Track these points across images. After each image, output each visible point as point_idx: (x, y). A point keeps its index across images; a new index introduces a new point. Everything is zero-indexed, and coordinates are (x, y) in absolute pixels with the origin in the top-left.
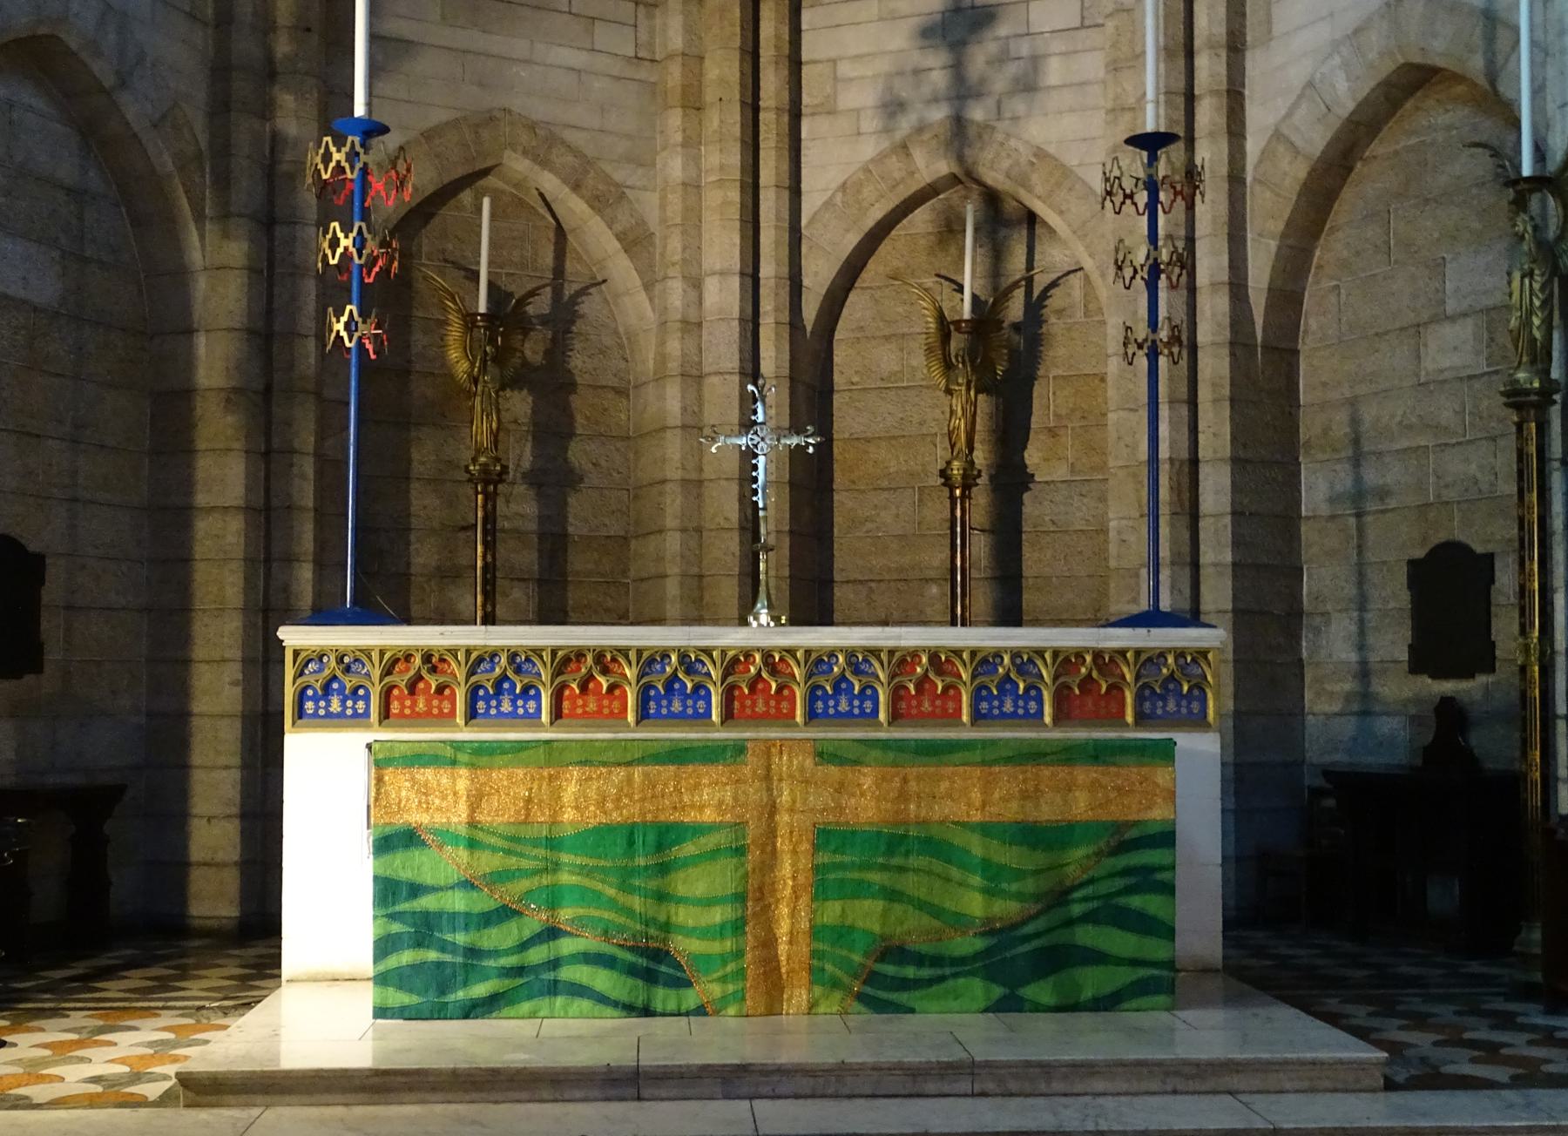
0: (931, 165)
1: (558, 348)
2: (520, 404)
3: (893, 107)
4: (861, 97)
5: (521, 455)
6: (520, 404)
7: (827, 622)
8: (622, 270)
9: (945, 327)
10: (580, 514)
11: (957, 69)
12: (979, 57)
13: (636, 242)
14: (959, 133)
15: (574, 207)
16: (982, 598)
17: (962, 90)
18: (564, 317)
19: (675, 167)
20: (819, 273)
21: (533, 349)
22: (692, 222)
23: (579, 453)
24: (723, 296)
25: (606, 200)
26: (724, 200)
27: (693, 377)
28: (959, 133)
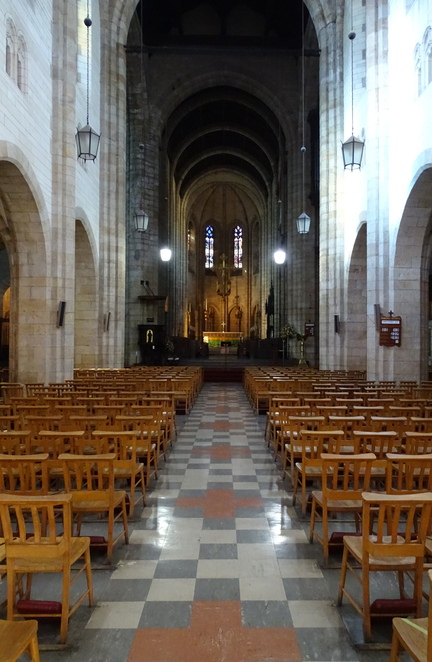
0: (235, 305)
1: (214, 316)
2: (212, 319)
3: (233, 301)
4: (231, 301)
5: (212, 322)
6: (212, 319)
7: (230, 331)
8: (217, 311)
9: (236, 315)
10: (215, 325)
11: (237, 300)
12: (238, 299)
13: (218, 309)
14: (237, 303)
15: (215, 308)
16: (238, 330)
17: (237, 301)
18: (214, 313)
19: (220, 305)
20: (229, 311)
21: (212, 315)
22: (222, 308)
23: (215, 322)
24: (223, 313)
25: (217, 307)
26: (223, 307)
27: (222, 317)
28: (237, 303)
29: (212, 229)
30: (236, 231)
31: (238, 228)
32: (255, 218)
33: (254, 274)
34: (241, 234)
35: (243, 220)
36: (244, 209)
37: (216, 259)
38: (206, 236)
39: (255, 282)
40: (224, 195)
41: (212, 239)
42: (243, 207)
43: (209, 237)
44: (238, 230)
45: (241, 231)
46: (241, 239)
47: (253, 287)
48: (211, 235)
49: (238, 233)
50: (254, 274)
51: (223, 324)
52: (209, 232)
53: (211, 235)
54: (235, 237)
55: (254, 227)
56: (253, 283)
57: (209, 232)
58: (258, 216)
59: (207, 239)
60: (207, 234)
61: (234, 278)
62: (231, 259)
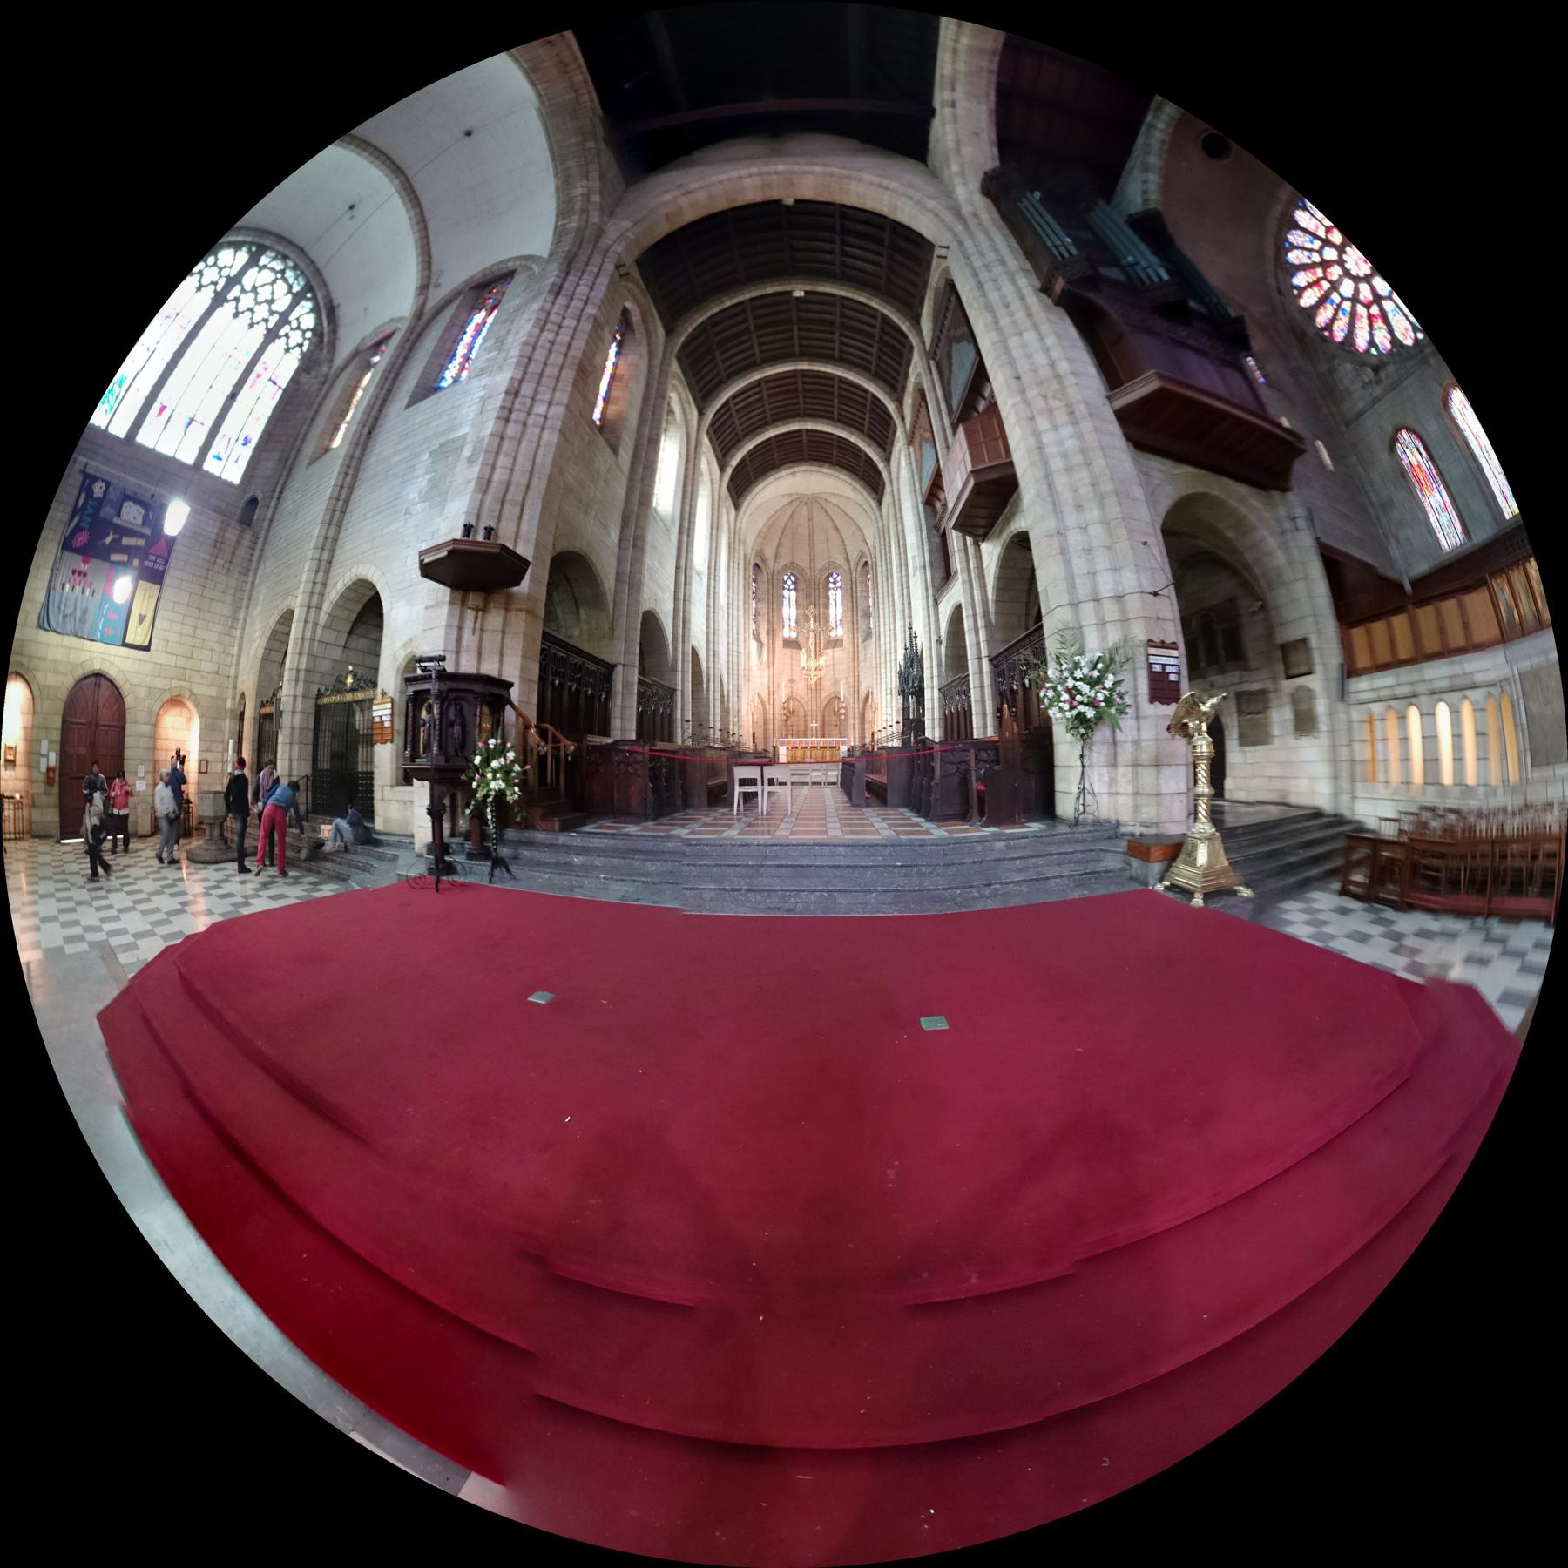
29: (793, 579)
30: (831, 579)
31: (835, 576)
32: (862, 554)
33: (864, 641)
34: (839, 584)
35: (841, 561)
36: (843, 541)
37: (801, 621)
38: (784, 588)
39: (866, 655)
40: (810, 519)
41: (793, 594)
42: (841, 537)
43: (789, 590)
44: (835, 579)
45: (838, 579)
46: (839, 592)
47: (862, 664)
48: (792, 587)
49: (835, 582)
50: (864, 641)
51: (814, 725)
52: (789, 582)
53: (792, 587)
54: (829, 589)
55: (859, 569)
56: (861, 657)
57: (789, 582)
58: (867, 553)
59: (786, 593)
60: (786, 586)
61: (830, 651)
62: (823, 619)
